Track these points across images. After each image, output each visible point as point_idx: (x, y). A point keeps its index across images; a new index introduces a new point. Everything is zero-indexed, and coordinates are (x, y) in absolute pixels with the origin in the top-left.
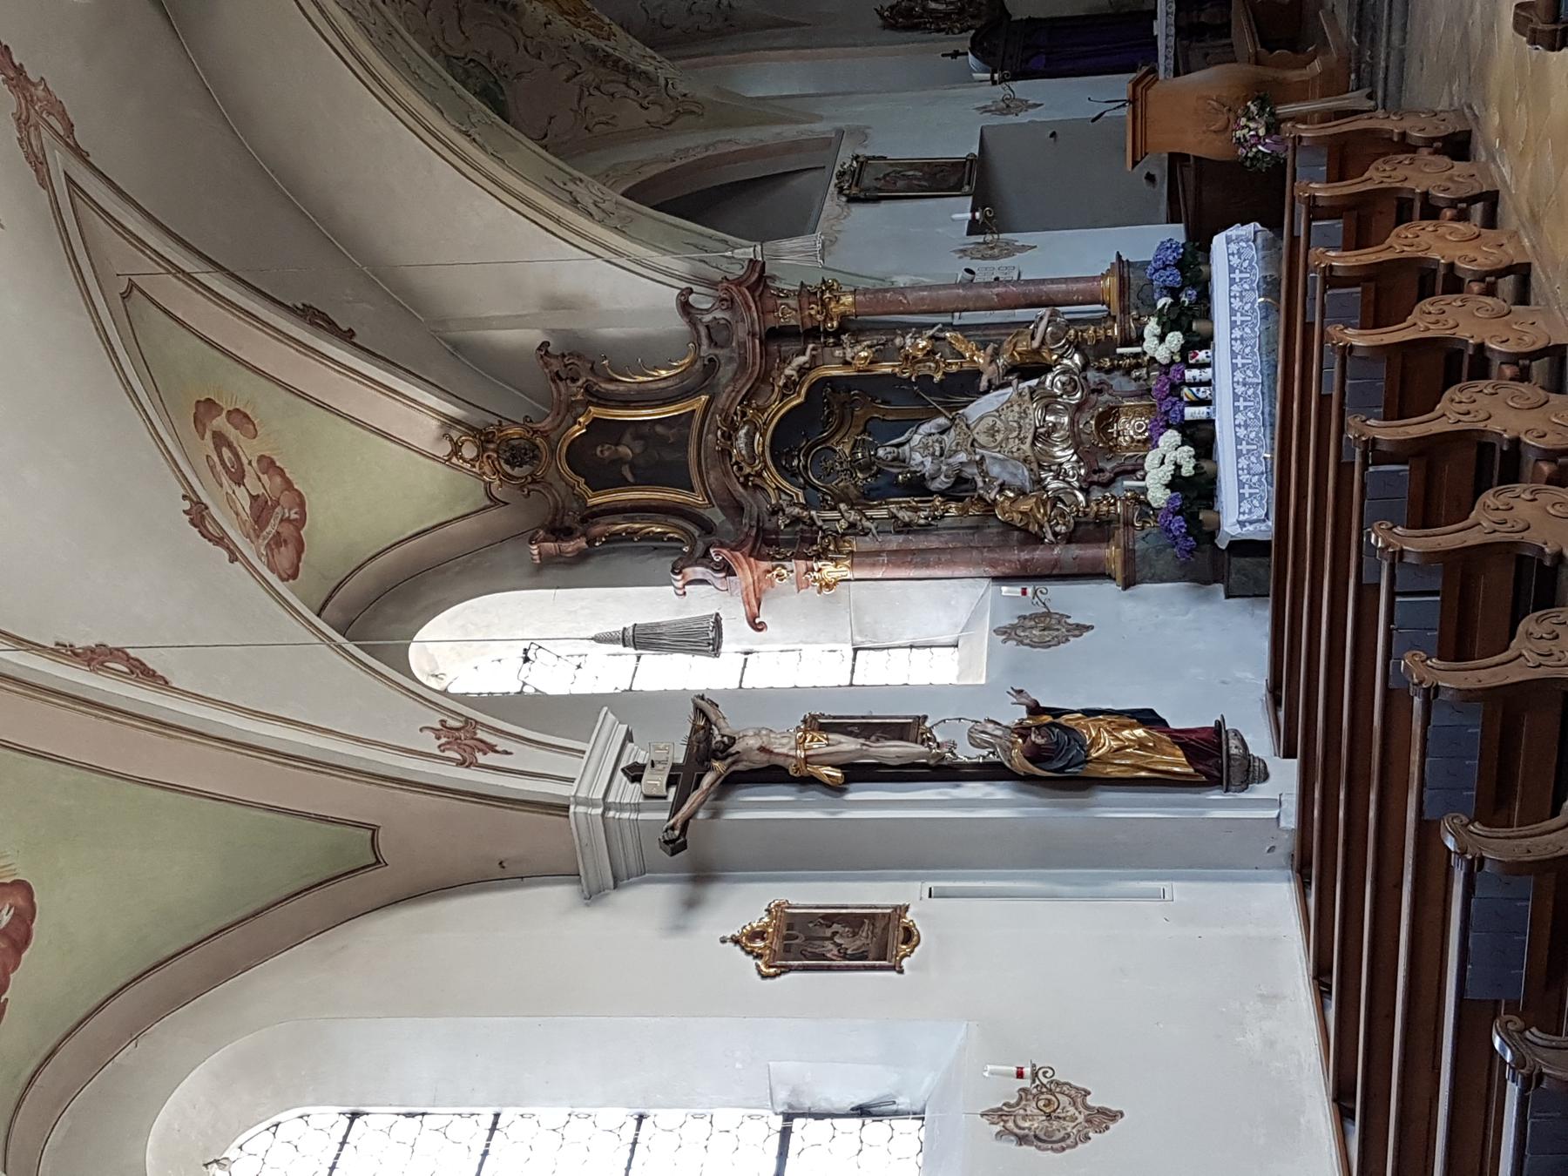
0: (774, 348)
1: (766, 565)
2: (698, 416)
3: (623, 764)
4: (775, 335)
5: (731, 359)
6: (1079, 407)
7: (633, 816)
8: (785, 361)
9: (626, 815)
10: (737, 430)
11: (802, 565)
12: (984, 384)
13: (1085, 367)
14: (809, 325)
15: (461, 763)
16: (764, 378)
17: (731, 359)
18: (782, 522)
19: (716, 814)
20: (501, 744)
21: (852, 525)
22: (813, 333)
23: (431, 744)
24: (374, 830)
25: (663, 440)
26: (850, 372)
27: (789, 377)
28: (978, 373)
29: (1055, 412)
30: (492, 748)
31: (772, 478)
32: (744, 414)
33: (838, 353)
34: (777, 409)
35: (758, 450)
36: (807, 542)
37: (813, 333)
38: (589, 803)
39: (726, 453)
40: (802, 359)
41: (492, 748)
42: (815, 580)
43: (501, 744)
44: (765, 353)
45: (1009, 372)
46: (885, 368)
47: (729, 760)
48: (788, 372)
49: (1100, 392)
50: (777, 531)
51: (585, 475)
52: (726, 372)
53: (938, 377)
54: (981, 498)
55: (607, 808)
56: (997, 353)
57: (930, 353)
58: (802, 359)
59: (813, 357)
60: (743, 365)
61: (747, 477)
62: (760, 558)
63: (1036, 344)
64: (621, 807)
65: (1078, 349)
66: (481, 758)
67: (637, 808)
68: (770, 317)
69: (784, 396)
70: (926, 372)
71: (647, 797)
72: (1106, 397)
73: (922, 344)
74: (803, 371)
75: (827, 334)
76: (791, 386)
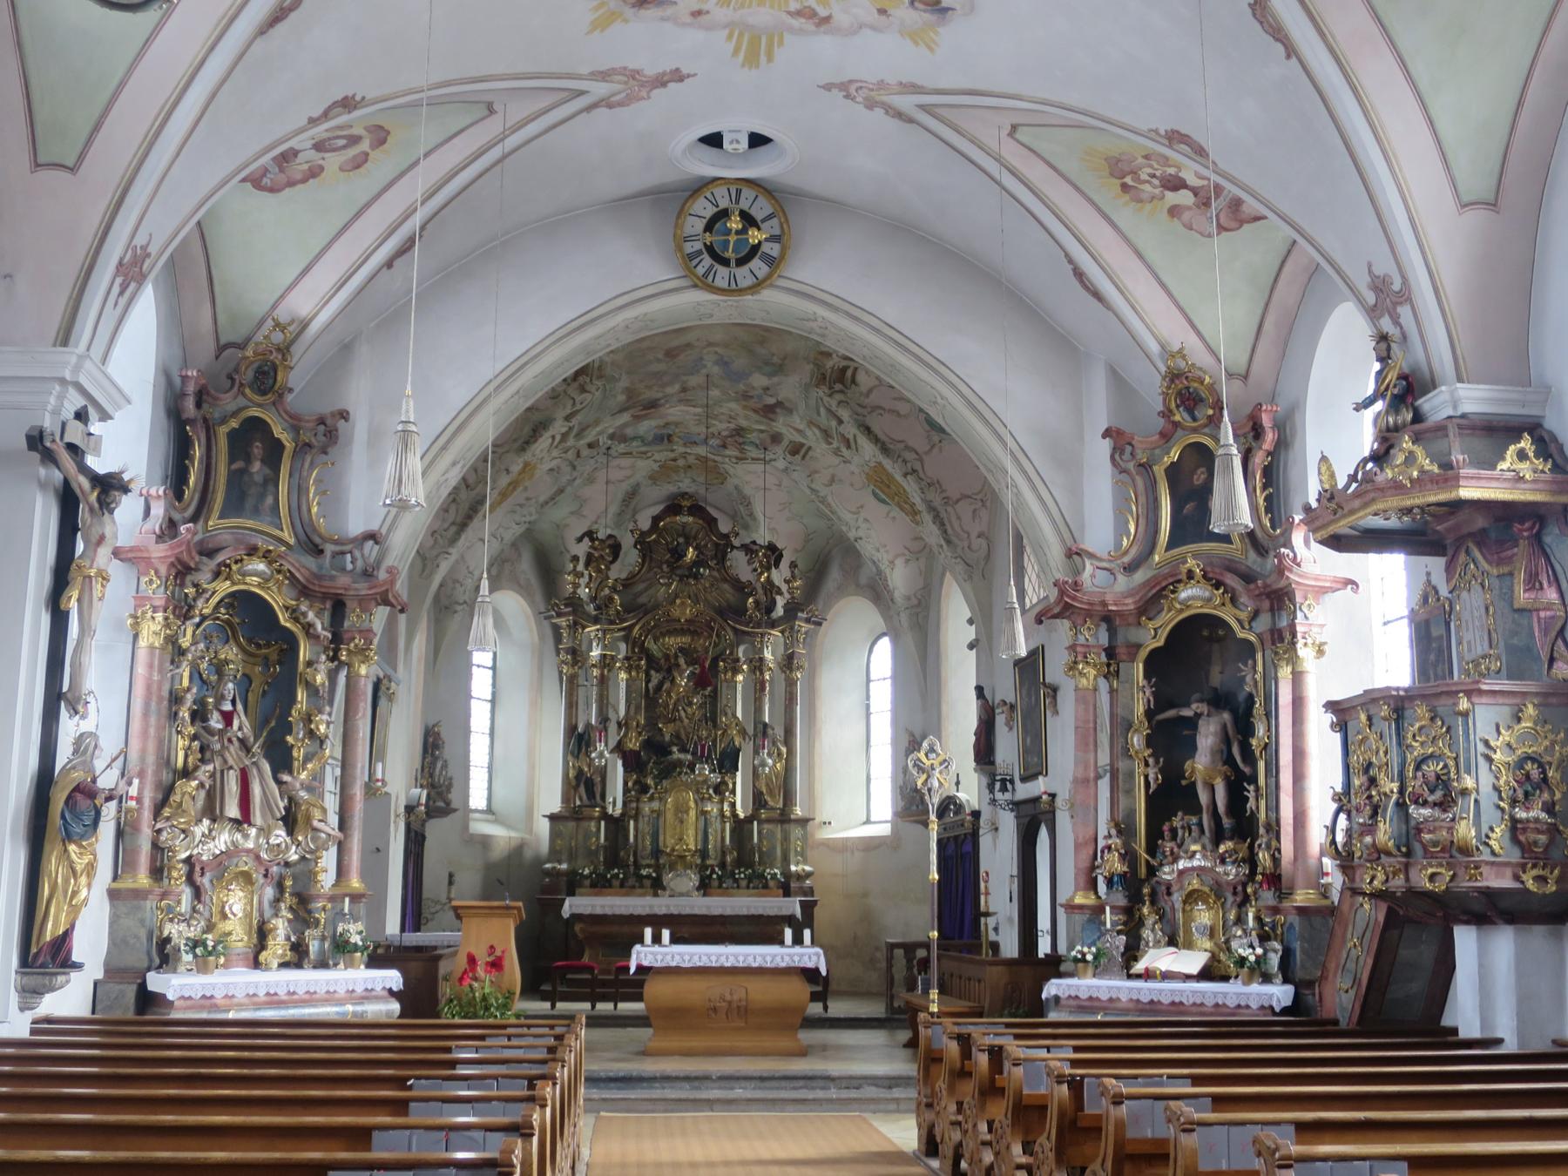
0: (328, 605)
1: (163, 570)
2: (277, 532)
3: (91, 410)
4: (338, 608)
5: (321, 567)
6: (258, 858)
7: (49, 408)
8: (318, 615)
9: (52, 400)
10: (270, 563)
11: (160, 602)
12: (286, 778)
13: (287, 864)
14: (346, 636)
15: (120, 264)
16: (304, 591)
17: (321, 567)
18: (190, 591)
19: (43, 486)
20: (123, 301)
21: (182, 652)
22: (337, 639)
23: (140, 240)
24: (72, 170)
25: (262, 496)
26: (301, 667)
27: (305, 615)
28: (290, 772)
29: (258, 837)
30: (121, 293)
31: (224, 588)
32: (279, 572)
33: (323, 657)
34: (277, 599)
35: (248, 579)
36: (181, 609)
37: (337, 639)
38: (77, 368)
39: (252, 551)
40: (319, 627)
41: (121, 293)
42: (144, 613)
43: (123, 301)
44: (325, 597)
45: (291, 799)
46: (301, 695)
47: (96, 505)
48: (311, 616)
49: (266, 876)
50: (182, 585)
51: (244, 422)
52: (310, 562)
53: (290, 739)
54: (196, 768)
55: (63, 381)
56: (309, 789)
57: (311, 734)
58: (319, 627)
59: (317, 637)
60: (319, 577)
61: (228, 566)
62: (172, 564)
63: (316, 823)
64: (61, 397)
65: (303, 858)
66: (119, 280)
67: (56, 412)
68: (355, 604)
69: (287, 608)
70: (295, 730)
71: (64, 425)
72: (261, 880)
73: (322, 728)
74: (308, 628)
75: (337, 651)
76: (295, 615)
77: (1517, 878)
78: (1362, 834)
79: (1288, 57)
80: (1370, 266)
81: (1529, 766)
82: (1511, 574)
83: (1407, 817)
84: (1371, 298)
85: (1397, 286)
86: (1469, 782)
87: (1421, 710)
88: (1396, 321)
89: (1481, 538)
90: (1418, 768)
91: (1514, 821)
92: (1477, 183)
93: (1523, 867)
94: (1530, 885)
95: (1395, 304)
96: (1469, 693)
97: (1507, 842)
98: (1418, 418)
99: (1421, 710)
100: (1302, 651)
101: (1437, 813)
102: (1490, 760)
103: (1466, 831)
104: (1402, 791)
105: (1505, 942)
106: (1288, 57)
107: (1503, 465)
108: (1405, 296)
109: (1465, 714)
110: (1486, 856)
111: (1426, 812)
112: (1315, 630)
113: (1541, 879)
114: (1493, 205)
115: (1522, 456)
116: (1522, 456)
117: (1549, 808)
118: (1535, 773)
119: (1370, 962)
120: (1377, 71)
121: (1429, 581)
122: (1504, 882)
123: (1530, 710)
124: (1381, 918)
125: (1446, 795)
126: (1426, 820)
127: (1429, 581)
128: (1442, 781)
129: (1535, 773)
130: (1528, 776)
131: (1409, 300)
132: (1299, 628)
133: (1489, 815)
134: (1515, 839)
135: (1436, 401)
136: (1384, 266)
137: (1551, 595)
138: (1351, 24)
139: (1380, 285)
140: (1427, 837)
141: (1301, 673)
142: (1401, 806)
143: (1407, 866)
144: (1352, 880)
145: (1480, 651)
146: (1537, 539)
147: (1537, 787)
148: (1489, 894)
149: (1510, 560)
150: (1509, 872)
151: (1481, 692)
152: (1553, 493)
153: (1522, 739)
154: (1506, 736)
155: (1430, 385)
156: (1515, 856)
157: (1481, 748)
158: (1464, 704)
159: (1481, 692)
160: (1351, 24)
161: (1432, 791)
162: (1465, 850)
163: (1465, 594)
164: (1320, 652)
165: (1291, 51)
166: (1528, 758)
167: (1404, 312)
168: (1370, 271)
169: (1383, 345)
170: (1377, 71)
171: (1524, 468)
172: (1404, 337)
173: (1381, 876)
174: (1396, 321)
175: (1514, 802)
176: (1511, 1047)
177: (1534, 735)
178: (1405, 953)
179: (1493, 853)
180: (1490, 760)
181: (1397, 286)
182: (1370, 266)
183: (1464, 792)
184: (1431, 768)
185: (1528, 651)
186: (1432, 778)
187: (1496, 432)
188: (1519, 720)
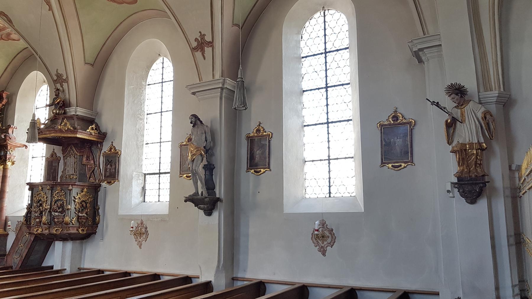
77: (77, 230)
78: (35, 219)
79: (49, 10)
80: (57, 70)
81: (83, 203)
82: (83, 156)
83: (51, 214)
84: (55, 78)
85: (64, 77)
86: (69, 207)
87: (59, 188)
88: (62, 86)
89: (76, 146)
90: (55, 203)
91: (78, 216)
92: (90, 60)
93: (79, 228)
94: (80, 232)
95: (63, 82)
96: (72, 185)
97: (76, 222)
98: (65, 113)
99: (59, 188)
100: (9, 164)
101: (60, 214)
102: (75, 201)
103: (67, 219)
104: (50, 208)
105: (69, 245)
106: (49, 10)
107: (88, 131)
108: (66, 81)
109: (71, 190)
110: (71, 225)
111: (56, 214)
112: (12, 157)
113: (83, 230)
114: (92, 65)
115: (92, 129)
116: (92, 129)
117: (86, 214)
118: (84, 205)
119: (27, 251)
120: (73, 23)
121: (54, 151)
122: (73, 231)
123: (85, 190)
124: (32, 239)
125: (63, 210)
126: (56, 216)
127: (54, 151)
128: (62, 206)
129: (84, 205)
130: (83, 205)
131: (67, 82)
132: (8, 157)
133: (73, 215)
134: (78, 221)
135: (71, 110)
136: (62, 71)
137: (92, 162)
138: (69, 9)
139: (59, 76)
140: (56, 220)
141: (7, 169)
142: (50, 212)
143: (49, 227)
144: (30, 230)
145: (71, 173)
146: (90, 148)
147: (85, 208)
148: (70, 234)
149: (83, 152)
150: (75, 229)
151: (75, 185)
152: (97, 138)
153: (82, 197)
154: (79, 196)
155: (69, 106)
156: (78, 225)
157: (73, 198)
158: (70, 188)
159: (75, 185)
160: (69, 9)
161: (59, 209)
162: (67, 224)
163: (68, 158)
164: (13, 163)
165: (51, 9)
166: (83, 201)
167: (65, 85)
168: (57, 71)
169: (58, 92)
170: (73, 23)
171: (92, 131)
172: (63, 91)
173: (40, 230)
174: (62, 86)
175: (79, 212)
176: (68, 272)
177: (85, 195)
178: (37, 248)
179: (73, 224)
180: (75, 201)
181: (64, 77)
182: (57, 70)
183: (68, 209)
184: (59, 203)
185: (84, 175)
186: (59, 205)
187: (88, 122)
188: (82, 192)
